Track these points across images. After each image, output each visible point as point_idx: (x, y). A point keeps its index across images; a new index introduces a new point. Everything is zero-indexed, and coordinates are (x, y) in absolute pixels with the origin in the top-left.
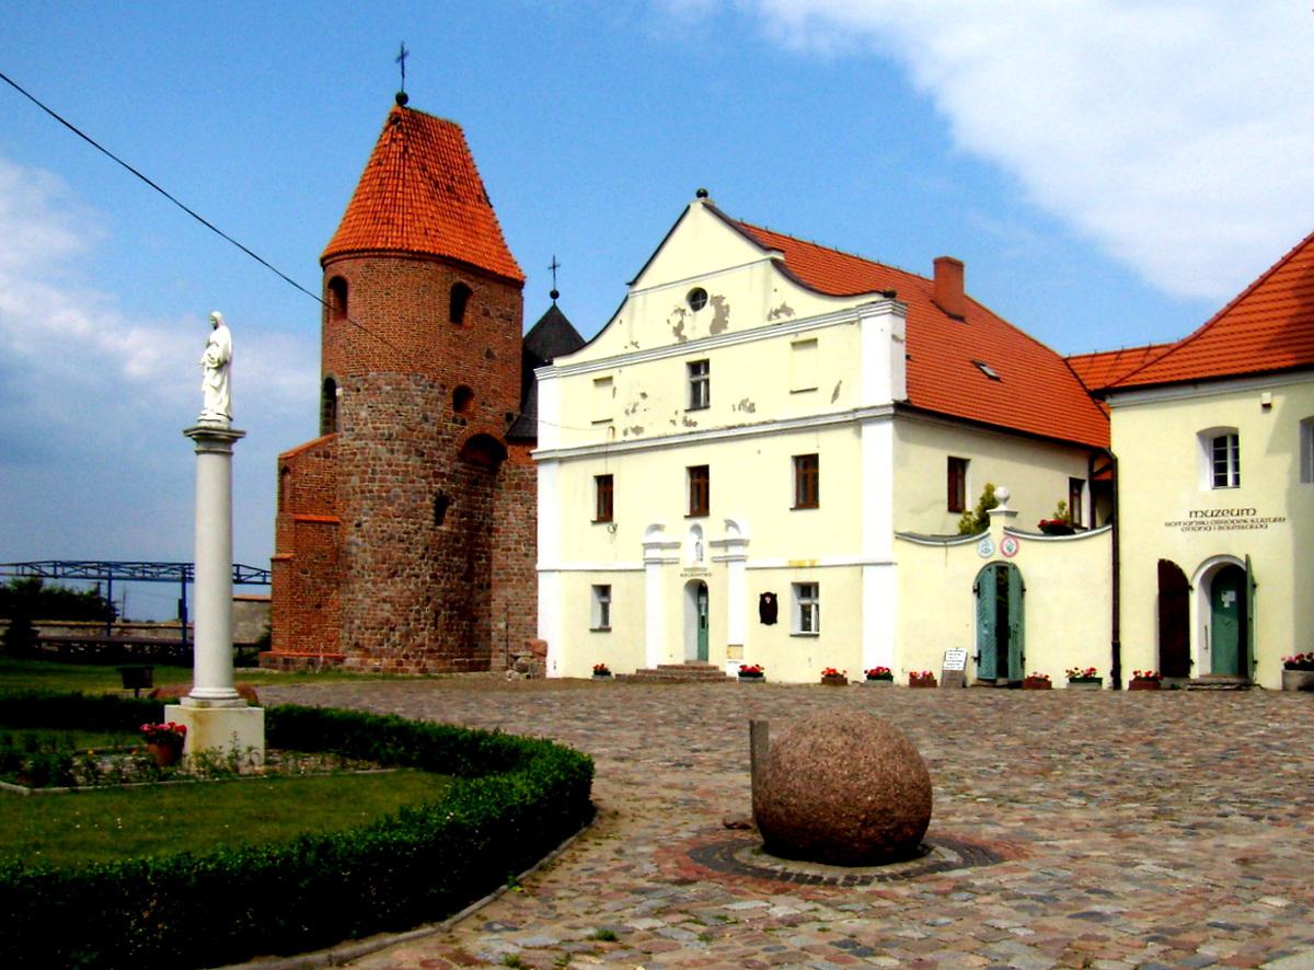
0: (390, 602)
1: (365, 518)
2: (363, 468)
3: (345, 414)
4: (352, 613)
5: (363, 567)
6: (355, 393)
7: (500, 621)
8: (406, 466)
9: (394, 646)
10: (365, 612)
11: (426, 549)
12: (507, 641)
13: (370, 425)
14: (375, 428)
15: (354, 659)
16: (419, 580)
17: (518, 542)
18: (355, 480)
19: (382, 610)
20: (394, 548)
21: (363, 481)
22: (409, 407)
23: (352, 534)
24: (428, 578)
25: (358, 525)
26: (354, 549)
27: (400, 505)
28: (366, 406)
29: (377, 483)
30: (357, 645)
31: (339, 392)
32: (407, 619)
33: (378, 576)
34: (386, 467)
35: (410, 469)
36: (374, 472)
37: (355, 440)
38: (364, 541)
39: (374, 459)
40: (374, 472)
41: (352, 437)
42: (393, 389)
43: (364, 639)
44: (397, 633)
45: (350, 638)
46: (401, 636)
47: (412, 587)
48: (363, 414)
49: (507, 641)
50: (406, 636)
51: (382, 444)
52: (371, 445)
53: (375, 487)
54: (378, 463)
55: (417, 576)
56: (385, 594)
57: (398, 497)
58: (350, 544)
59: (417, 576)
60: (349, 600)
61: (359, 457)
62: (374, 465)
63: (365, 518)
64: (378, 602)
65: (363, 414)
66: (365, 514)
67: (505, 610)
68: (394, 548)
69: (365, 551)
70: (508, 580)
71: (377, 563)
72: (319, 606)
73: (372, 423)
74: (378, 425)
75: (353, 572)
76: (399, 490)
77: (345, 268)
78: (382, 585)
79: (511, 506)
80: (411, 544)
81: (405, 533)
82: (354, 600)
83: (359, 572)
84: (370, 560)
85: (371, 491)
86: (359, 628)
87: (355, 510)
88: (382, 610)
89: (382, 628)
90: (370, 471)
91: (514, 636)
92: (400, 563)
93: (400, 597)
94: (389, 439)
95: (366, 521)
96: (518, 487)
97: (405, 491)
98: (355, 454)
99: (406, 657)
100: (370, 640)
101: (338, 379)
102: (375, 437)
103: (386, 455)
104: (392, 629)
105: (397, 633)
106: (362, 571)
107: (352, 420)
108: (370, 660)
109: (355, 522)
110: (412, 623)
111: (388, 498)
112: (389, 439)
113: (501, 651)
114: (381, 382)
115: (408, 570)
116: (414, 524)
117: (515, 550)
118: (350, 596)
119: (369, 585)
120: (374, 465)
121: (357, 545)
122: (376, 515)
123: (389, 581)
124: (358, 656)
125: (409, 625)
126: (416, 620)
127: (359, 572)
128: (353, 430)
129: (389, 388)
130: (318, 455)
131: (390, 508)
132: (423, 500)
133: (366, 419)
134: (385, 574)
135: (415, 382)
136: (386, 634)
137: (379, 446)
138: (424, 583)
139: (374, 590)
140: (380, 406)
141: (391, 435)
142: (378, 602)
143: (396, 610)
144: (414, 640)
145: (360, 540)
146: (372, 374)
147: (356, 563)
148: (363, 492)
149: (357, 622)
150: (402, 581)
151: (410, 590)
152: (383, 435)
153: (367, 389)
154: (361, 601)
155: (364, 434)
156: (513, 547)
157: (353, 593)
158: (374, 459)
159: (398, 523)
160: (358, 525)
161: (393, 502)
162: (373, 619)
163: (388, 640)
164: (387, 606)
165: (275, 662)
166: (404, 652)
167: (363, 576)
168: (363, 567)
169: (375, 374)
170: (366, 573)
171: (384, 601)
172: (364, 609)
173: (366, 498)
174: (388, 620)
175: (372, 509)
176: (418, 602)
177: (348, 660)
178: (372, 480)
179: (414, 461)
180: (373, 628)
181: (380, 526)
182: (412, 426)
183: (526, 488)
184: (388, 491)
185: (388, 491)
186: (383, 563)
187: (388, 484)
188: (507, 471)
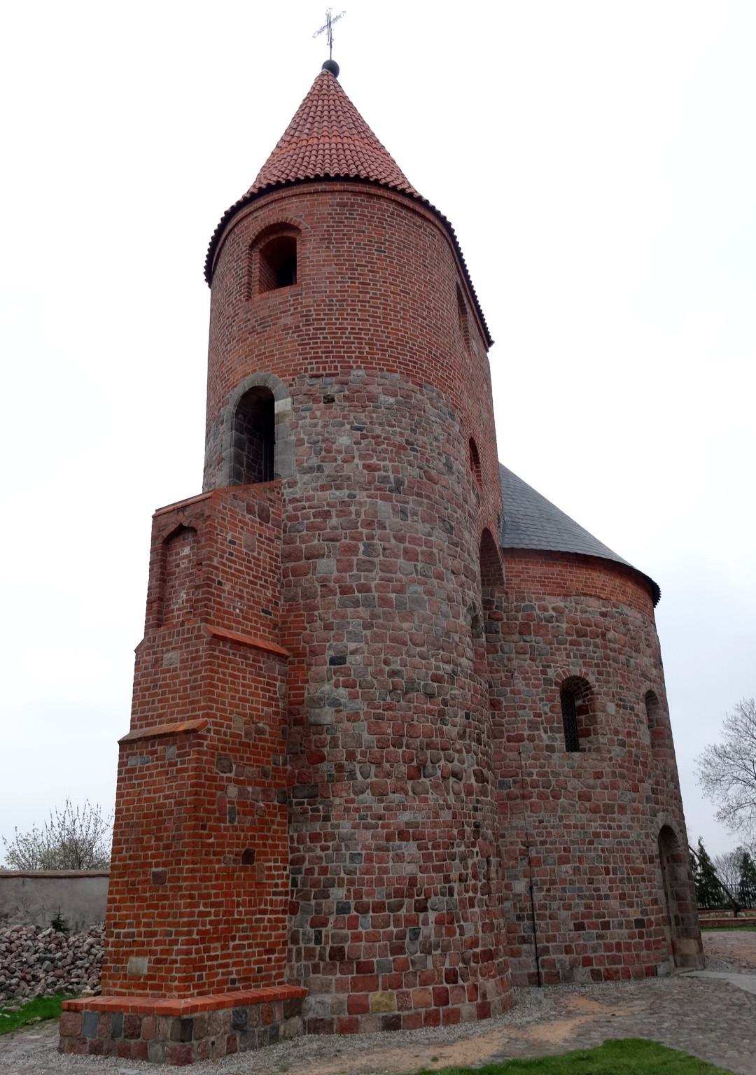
0: (415, 839)
3: (300, 442)
4: (324, 871)
5: (351, 756)
6: (322, 405)
7: (516, 878)
8: (429, 544)
9: (427, 951)
10: (360, 865)
11: (467, 717)
12: (532, 918)
13: (357, 461)
14: (367, 467)
15: (328, 999)
16: (462, 783)
17: (533, 726)
18: (328, 566)
19: (400, 858)
20: (418, 710)
21: (345, 567)
22: (425, 439)
23: (321, 681)
24: (473, 781)
25: (338, 660)
26: (327, 715)
27: (424, 619)
28: (348, 427)
30: (337, 954)
31: (282, 405)
32: (447, 879)
33: (389, 775)
34: (393, 541)
35: (435, 551)
36: (369, 549)
37: (323, 488)
38: (353, 697)
39: (369, 524)
40: (369, 549)
42: (397, 402)
43: (357, 938)
44: (432, 916)
45: (318, 941)
46: (439, 922)
47: (451, 799)
49: (532, 918)
50: (448, 921)
51: (384, 498)
52: (361, 496)
53: (375, 581)
54: (379, 532)
55: (457, 775)
56: (406, 817)
57: (418, 602)
58: (317, 702)
59: (457, 775)
60: (315, 837)
61: (334, 521)
62: (371, 537)
63: (352, 646)
64: (389, 838)
65: (344, 440)
66: (355, 637)
67: (525, 854)
68: (418, 710)
69: (354, 718)
70: (524, 797)
71: (382, 745)
72: (248, 857)
73: (362, 457)
74: (374, 461)
76: (420, 589)
77: (291, 209)
78: (397, 797)
79: (515, 663)
80: (445, 703)
81: (437, 679)
82: (332, 837)
84: (366, 736)
85: (365, 589)
86: (343, 909)
87: (328, 627)
88: (400, 858)
89: (400, 906)
90: (362, 548)
91: (544, 907)
92: (429, 746)
93: (436, 825)
94: (397, 489)
95: (352, 653)
96: (524, 630)
97: (430, 593)
98: (327, 515)
99: (452, 977)
100: (372, 938)
101: (278, 385)
102: (370, 483)
103: (393, 521)
104: (421, 908)
105: (432, 916)
106: (348, 766)
107: (318, 453)
108: (375, 997)
109: (331, 653)
110: (456, 886)
111: (401, 605)
112: (397, 489)
113: (524, 940)
114: (375, 389)
115: (442, 763)
116: (448, 662)
117: (531, 739)
118: (317, 827)
119: (367, 797)
120: (371, 537)
121: (335, 703)
122: (377, 638)
123: (410, 783)
124: (341, 987)
125: (451, 895)
126: (462, 879)
127: (340, 768)
129: (392, 400)
130: (250, 510)
131: (405, 625)
132: (456, 616)
133: (348, 450)
134: (404, 769)
135: (431, 399)
136: (410, 921)
137: (379, 502)
138: (469, 792)
139: (379, 808)
140: (378, 430)
141: (399, 483)
142: (389, 838)
143: (428, 858)
144: (461, 927)
145: (343, 692)
146: (358, 373)
148: (345, 590)
149: (338, 893)
150: (436, 787)
151: (449, 808)
152: (385, 480)
153: (346, 398)
154: (351, 837)
155: (349, 478)
156: (526, 733)
158: (369, 524)
159: (422, 657)
160: (338, 660)
161: (412, 612)
162: (380, 882)
163: (415, 934)
164: (410, 848)
165: (134, 1032)
166: (447, 966)
167: (352, 776)
168: (351, 756)
169: (361, 372)
170: (357, 767)
171: (403, 836)
173: (356, 604)
174: (413, 881)
175: (367, 626)
176: (462, 834)
177: (311, 1000)
178: (367, 566)
179: (439, 536)
180: (379, 907)
181: (386, 663)
182: (433, 472)
183: (537, 634)
184: (400, 591)
185: (400, 591)
186: (397, 745)
187: (399, 575)
188: (504, 604)
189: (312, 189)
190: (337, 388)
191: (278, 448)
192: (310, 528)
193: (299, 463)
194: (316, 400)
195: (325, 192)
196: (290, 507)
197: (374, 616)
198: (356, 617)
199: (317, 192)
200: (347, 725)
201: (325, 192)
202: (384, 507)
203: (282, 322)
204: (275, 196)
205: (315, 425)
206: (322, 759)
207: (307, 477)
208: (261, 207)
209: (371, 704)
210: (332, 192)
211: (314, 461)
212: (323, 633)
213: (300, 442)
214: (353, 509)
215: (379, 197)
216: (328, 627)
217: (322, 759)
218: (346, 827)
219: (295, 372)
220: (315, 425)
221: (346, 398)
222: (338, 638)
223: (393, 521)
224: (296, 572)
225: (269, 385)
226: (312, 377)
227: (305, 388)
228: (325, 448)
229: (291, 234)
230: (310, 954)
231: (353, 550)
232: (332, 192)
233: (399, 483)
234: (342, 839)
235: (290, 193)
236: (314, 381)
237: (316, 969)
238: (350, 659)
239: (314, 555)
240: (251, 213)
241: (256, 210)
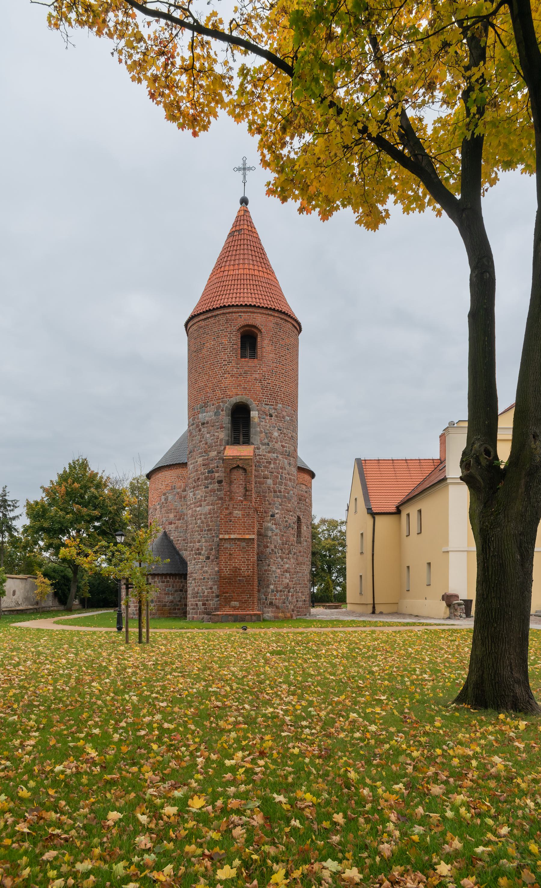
1: (277, 511)
2: (275, 474)
5: (275, 547)
18: (270, 481)
23: (268, 522)
25: (273, 516)
26: (270, 533)
29: (283, 487)
30: (271, 603)
31: (254, 414)
37: (269, 452)
38: (276, 528)
41: (267, 450)
45: (266, 600)
48: (276, 434)
52: (280, 457)
58: (267, 529)
61: (272, 466)
63: (277, 511)
65: (276, 434)
66: (277, 508)
73: (281, 442)
74: (284, 444)
75: (268, 549)
76: (292, 492)
83: (272, 550)
85: (280, 492)
86: (273, 591)
87: (270, 504)
94: (288, 455)
101: (253, 404)
103: (287, 467)
118: (266, 568)
119: (279, 559)
120: (282, 473)
121: (272, 530)
122: (283, 509)
124: (272, 612)
127: (272, 550)
128: (268, 444)
141: (289, 452)
145: (274, 526)
147: (271, 543)
148: (275, 492)
149: (272, 587)
152: (286, 451)
157: (269, 565)
158: (282, 468)
160: (273, 516)
167: (275, 553)
169: (281, 405)
172: (276, 577)
178: (281, 484)
185: (288, 493)
189: (267, 312)
190: (273, 411)
191: (252, 430)
192: (265, 467)
193: (261, 441)
194: (266, 415)
195: (271, 315)
196: (258, 457)
197: (282, 502)
198: (278, 501)
199: (268, 314)
200: (275, 537)
201: (271, 315)
202: (286, 461)
203: (254, 376)
204: (251, 310)
205: (266, 426)
206: (268, 547)
207: (264, 447)
208: (244, 312)
209: (281, 530)
210: (274, 316)
211: (266, 441)
212: (269, 506)
213: (261, 432)
214: (278, 462)
215: (288, 321)
216: (270, 504)
217: (268, 547)
218: (274, 568)
219: (259, 401)
220: (266, 426)
221: (276, 416)
222: (272, 508)
223: (287, 467)
224: (260, 483)
225: (249, 403)
226: (266, 404)
227: (263, 409)
228: (269, 435)
229: (255, 331)
230: (264, 603)
231: (277, 477)
232: (274, 316)
233: (289, 452)
234: (273, 571)
235: (258, 311)
236: (267, 406)
237: (265, 607)
238: (276, 516)
239: (266, 477)
240: (238, 312)
241: (241, 312)
